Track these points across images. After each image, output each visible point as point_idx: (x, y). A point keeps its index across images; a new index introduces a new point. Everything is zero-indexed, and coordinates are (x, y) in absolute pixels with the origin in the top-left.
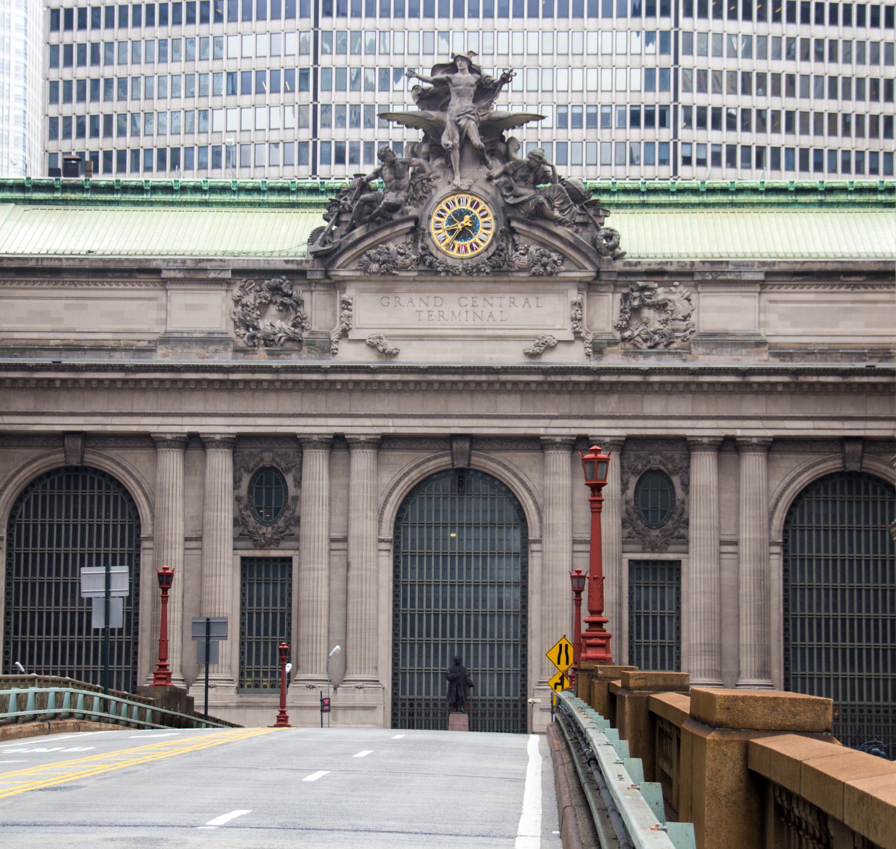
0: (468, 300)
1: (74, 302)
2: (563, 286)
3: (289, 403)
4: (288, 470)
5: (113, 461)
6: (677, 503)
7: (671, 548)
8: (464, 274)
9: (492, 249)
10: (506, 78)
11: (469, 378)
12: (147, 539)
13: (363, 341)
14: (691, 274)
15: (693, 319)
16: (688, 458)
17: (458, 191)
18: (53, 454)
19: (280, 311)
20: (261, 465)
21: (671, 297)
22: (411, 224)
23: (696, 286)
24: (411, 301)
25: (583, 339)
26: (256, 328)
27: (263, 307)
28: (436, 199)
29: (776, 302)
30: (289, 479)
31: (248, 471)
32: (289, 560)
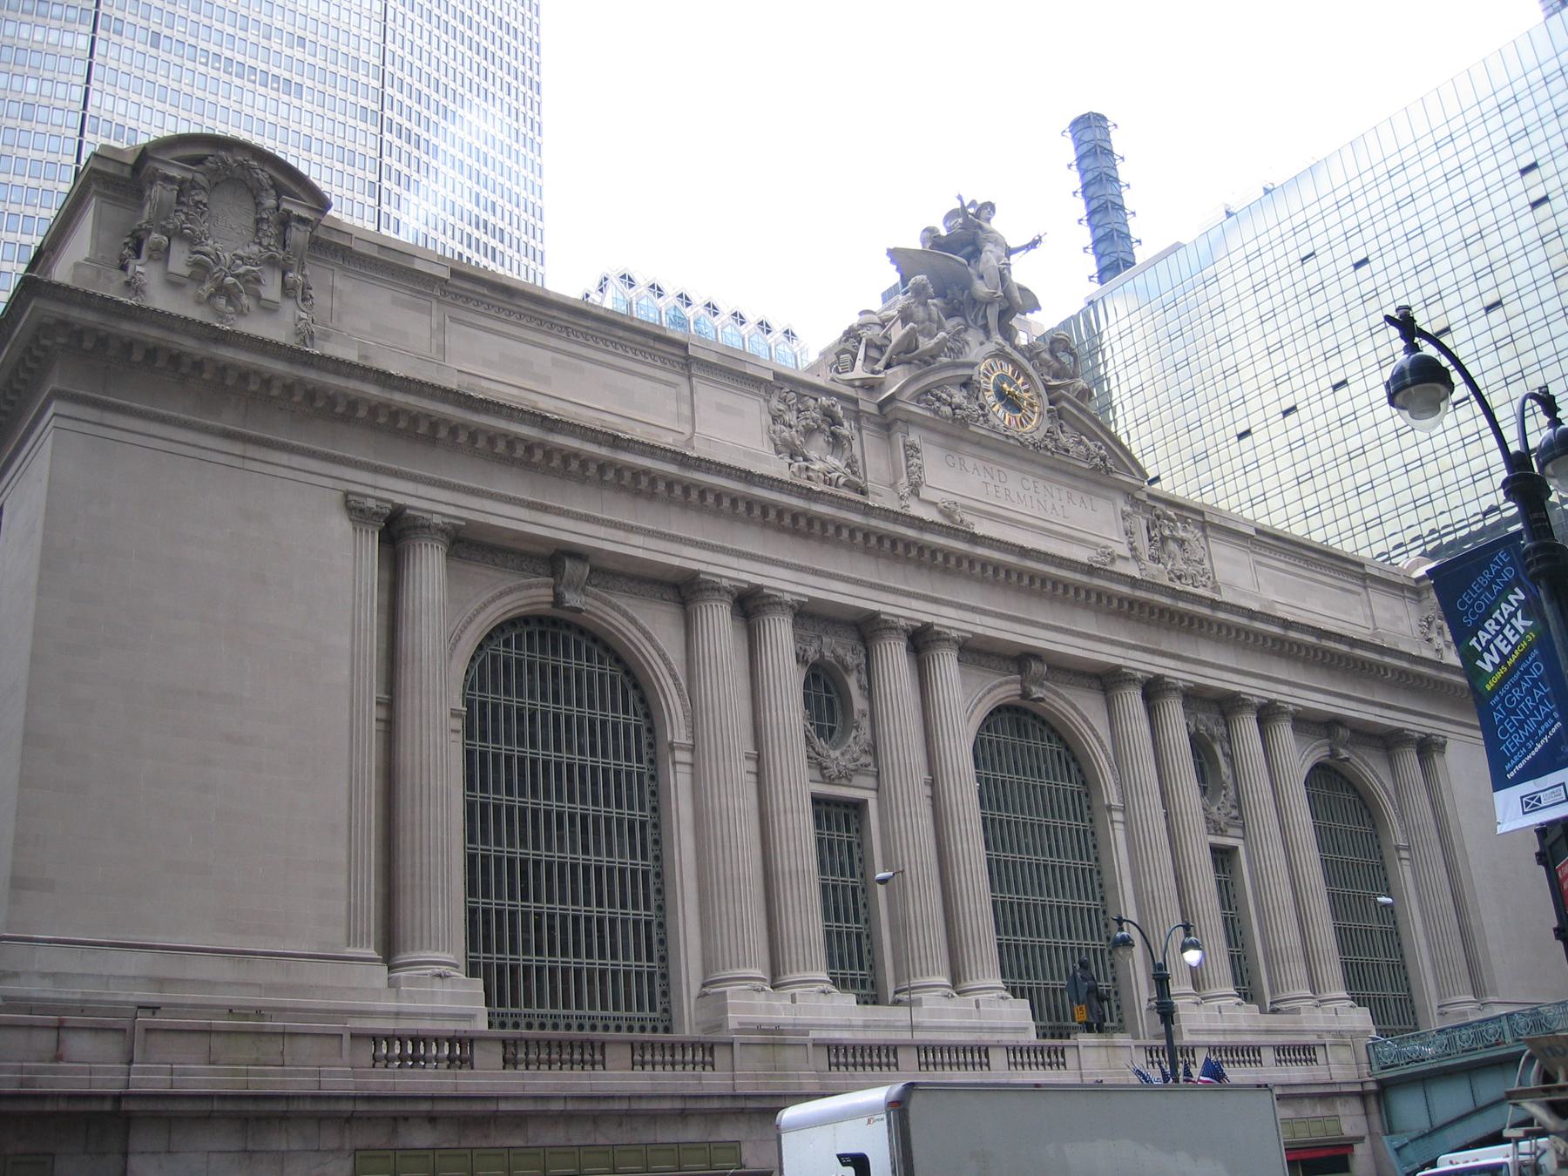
0: (1029, 484)
1: (565, 358)
2: (1112, 494)
3: (865, 569)
5: (625, 614)
7: (1231, 831)
9: (1043, 432)
10: (1034, 244)
13: (935, 504)
15: (1207, 565)
18: (537, 586)
23: (1203, 530)
25: (1136, 558)
27: (809, 432)
29: (1259, 563)
30: (852, 683)
32: (859, 806)
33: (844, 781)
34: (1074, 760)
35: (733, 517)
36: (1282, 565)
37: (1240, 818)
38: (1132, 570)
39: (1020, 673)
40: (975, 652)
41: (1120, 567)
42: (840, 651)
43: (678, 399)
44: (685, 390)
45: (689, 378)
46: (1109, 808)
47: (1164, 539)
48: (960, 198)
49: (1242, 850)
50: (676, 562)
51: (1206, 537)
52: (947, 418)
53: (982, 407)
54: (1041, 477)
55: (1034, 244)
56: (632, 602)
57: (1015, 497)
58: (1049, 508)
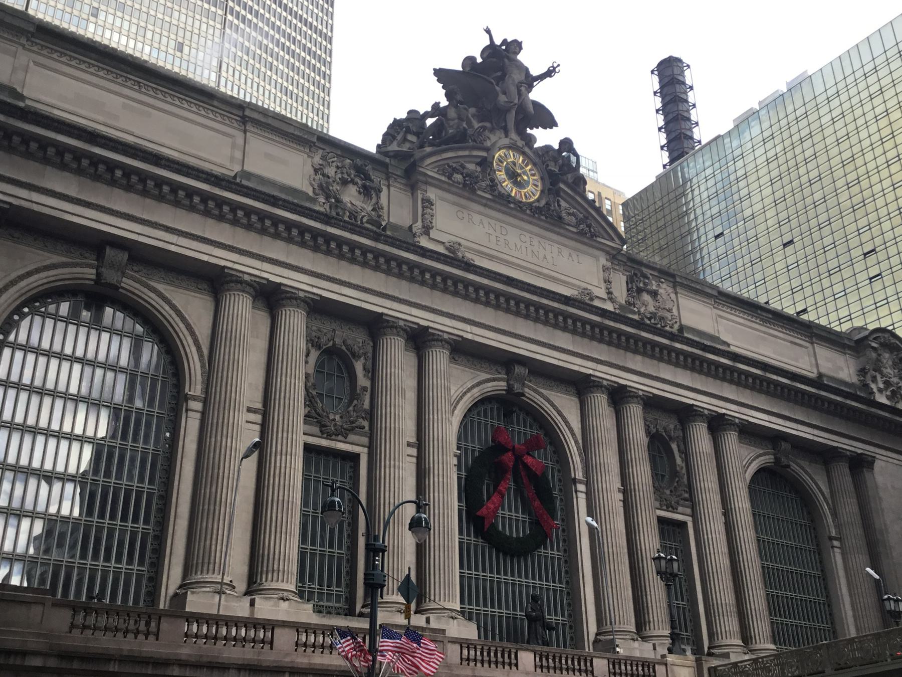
0: (527, 237)
1: (135, 104)
4: (356, 356)
6: (678, 469)
7: (680, 509)
8: (528, 212)
9: (543, 203)
10: (550, 73)
11: (545, 301)
12: (195, 398)
13: (443, 243)
14: (673, 276)
16: (684, 430)
17: (512, 147)
19: (360, 193)
20: (331, 344)
21: (661, 291)
22: (484, 154)
23: (674, 287)
24: (481, 222)
25: (611, 299)
26: (338, 201)
27: (344, 183)
28: (498, 145)
30: (359, 366)
31: (318, 346)
33: (340, 438)
34: (551, 444)
35: (263, 231)
36: (741, 321)
37: (689, 497)
38: (609, 307)
39: (507, 374)
40: (465, 352)
41: (596, 303)
42: (349, 342)
43: (234, 146)
44: (240, 141)
45: (245, 132)
46: (575, 481)
47: (640, 291)
48: (488, 31)
49: (690, 525)
50: (205, 258)
51: (676, 293)
52: (459, 183)
53: (492, 180)
54: (536, 235)
55: (550, 73)
56: (168, 287)
57: (513, 247)
58: (541, 256)
